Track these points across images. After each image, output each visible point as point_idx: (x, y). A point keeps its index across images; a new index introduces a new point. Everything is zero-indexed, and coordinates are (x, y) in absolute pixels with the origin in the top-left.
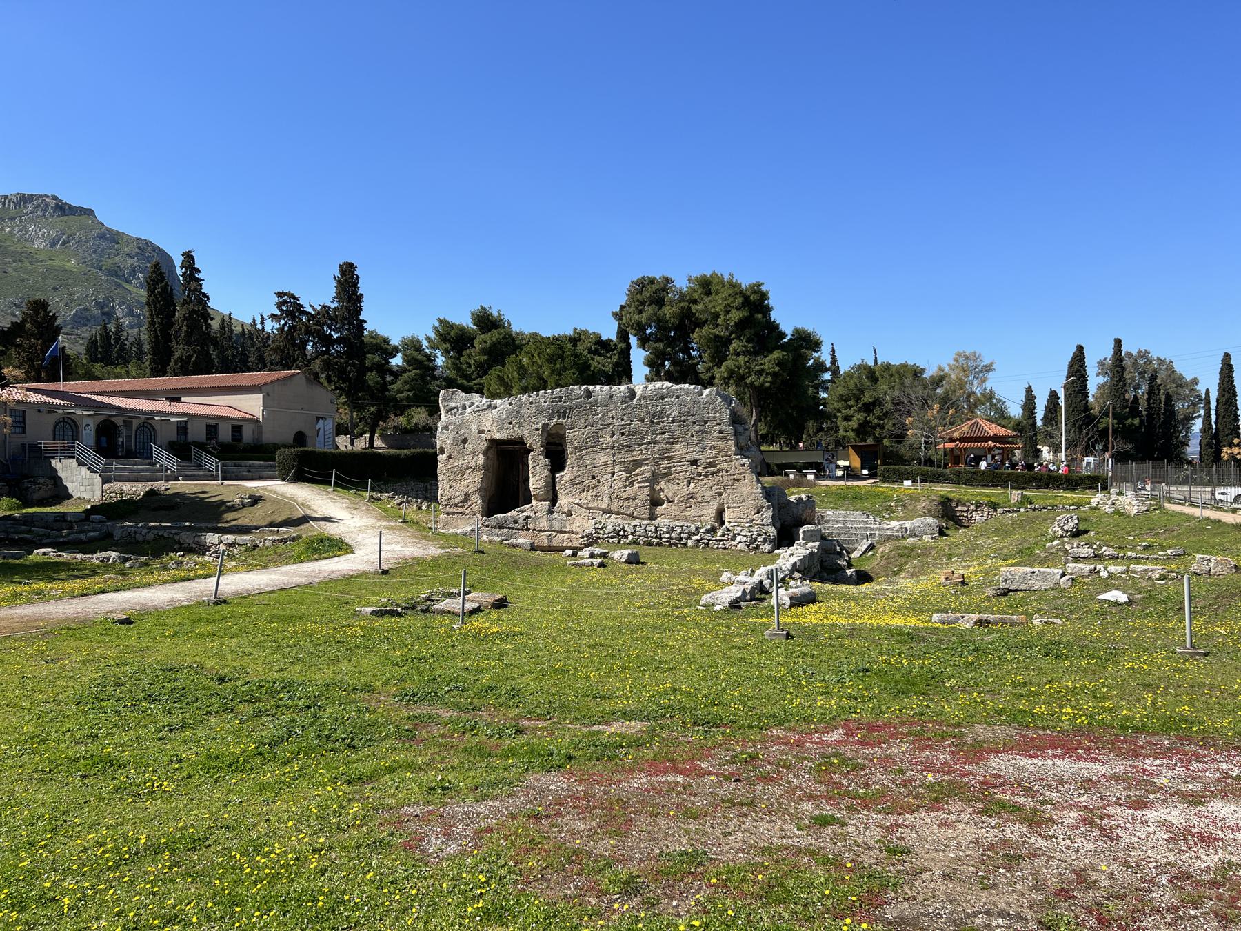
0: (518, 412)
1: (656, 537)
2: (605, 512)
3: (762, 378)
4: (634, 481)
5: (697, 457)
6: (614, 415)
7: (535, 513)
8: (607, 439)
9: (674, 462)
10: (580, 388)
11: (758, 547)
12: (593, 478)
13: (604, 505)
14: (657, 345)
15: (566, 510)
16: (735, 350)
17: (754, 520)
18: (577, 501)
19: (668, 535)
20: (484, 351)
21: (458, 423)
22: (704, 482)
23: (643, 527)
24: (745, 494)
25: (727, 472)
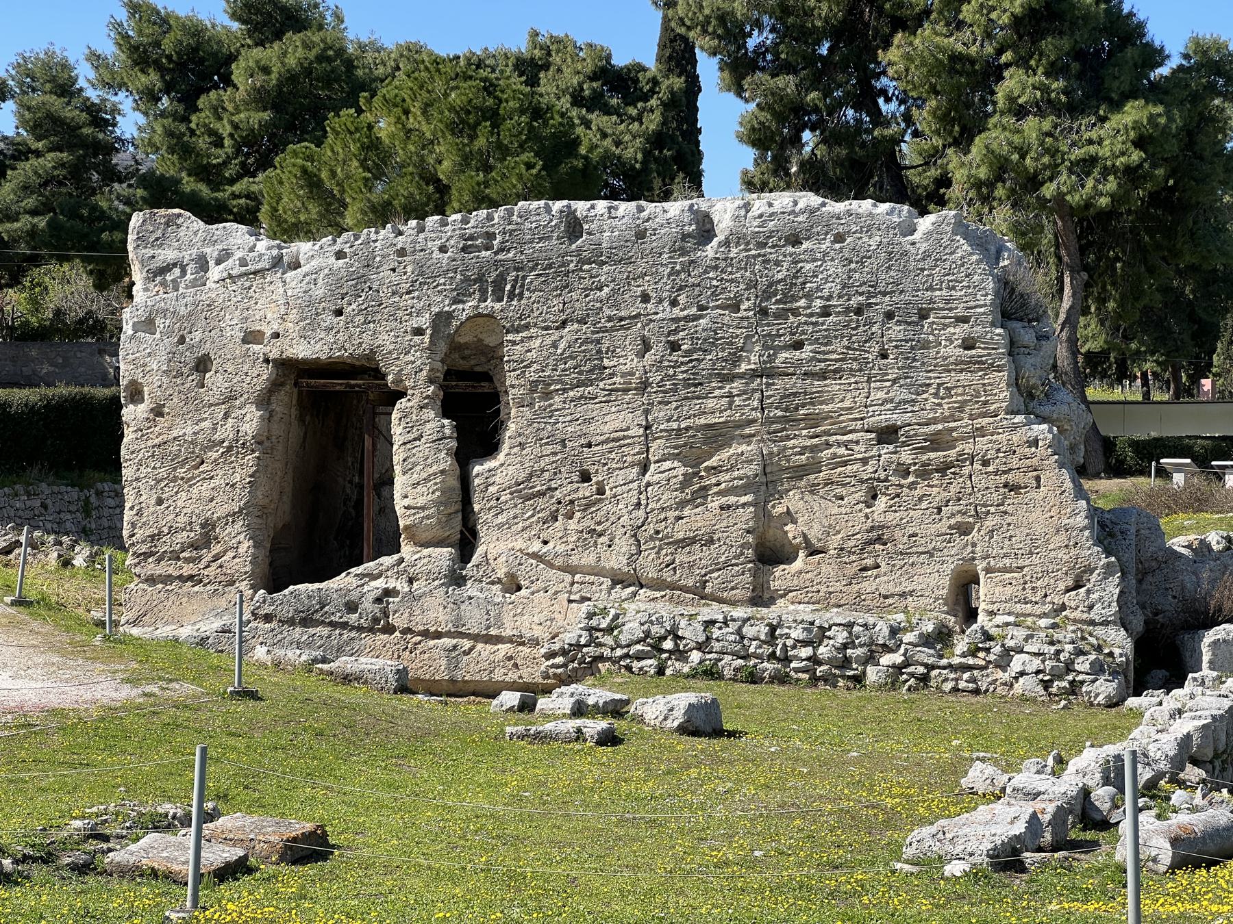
0: (362, 279)
1: (772, 656)
2: (618, 580)
3: (1090, 183)
4: (705, 488)
5: (897, 418)
6: (650, 289)
7: (410, 581)
8: (628, 362)
10: (548, 210)
11: (1074, 688)
13: (616, 560)
14: (780, 81)
15: (501, 573)
16: (1011, 99)
17: (1063, 607)
18: (536, 547)
19: (806, 652)
20: (260, 98)
21: (183, 311)
22: (919, 492)
23: (733, 627)
24: (1039, 529)
25: (986, 463)
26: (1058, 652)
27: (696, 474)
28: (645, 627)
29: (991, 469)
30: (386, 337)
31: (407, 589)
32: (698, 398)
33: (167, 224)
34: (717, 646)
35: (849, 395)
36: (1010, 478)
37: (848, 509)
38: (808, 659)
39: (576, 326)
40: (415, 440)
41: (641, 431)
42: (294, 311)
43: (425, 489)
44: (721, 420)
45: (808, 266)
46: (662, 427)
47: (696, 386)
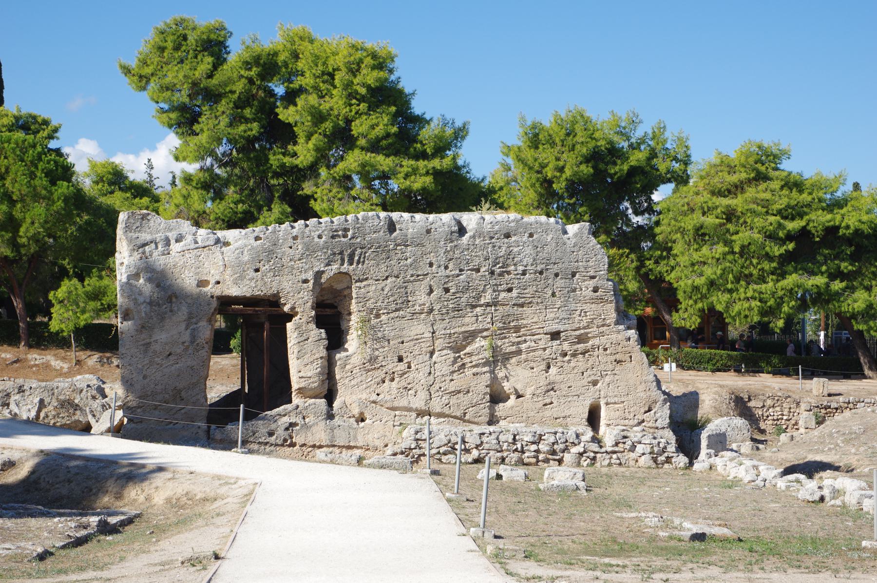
0: (271, 252)
2: (421, 414)
8: (421, 298)
9: (524, 335)
11: (668, 460)
12: (400, 359)
13: (418, 403)
17: (643, 421)
18: (374, 397)
23: (494, 436)
25: (606, 350)
26: (659, 443)
27: (459, 357)
28: (448, 438)
29: (608, 352)
30: (287, 284)
31: (303, 423)
32: (460, 317)
33: (142, 219)
34: (486, 446)
35: (536, 316)
36: (618, 357)
37: (537, 374)
38: (535, 451)
39: (394, 279)
40: (305, 340)
41: (431, 335)
42: (229, 269)
43: (312, 367)
44: (472, 329)
45: (516, 249)
46: (441, 333)
47: (458, 311)
